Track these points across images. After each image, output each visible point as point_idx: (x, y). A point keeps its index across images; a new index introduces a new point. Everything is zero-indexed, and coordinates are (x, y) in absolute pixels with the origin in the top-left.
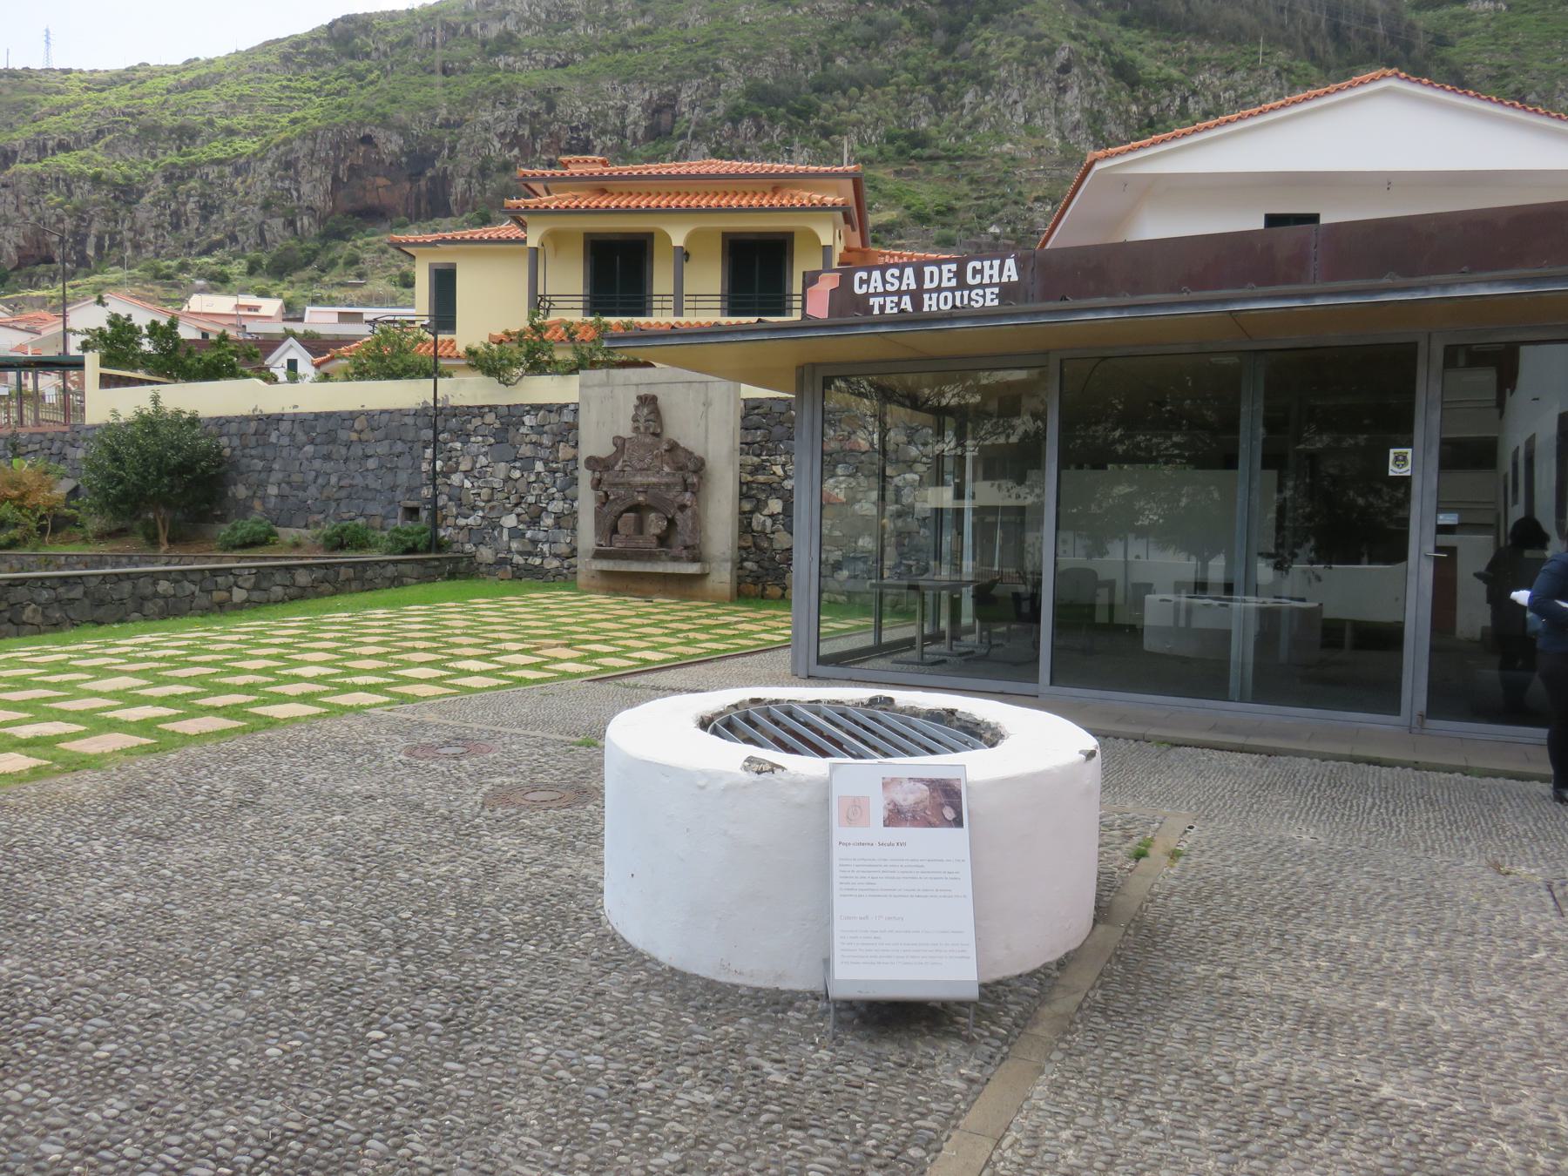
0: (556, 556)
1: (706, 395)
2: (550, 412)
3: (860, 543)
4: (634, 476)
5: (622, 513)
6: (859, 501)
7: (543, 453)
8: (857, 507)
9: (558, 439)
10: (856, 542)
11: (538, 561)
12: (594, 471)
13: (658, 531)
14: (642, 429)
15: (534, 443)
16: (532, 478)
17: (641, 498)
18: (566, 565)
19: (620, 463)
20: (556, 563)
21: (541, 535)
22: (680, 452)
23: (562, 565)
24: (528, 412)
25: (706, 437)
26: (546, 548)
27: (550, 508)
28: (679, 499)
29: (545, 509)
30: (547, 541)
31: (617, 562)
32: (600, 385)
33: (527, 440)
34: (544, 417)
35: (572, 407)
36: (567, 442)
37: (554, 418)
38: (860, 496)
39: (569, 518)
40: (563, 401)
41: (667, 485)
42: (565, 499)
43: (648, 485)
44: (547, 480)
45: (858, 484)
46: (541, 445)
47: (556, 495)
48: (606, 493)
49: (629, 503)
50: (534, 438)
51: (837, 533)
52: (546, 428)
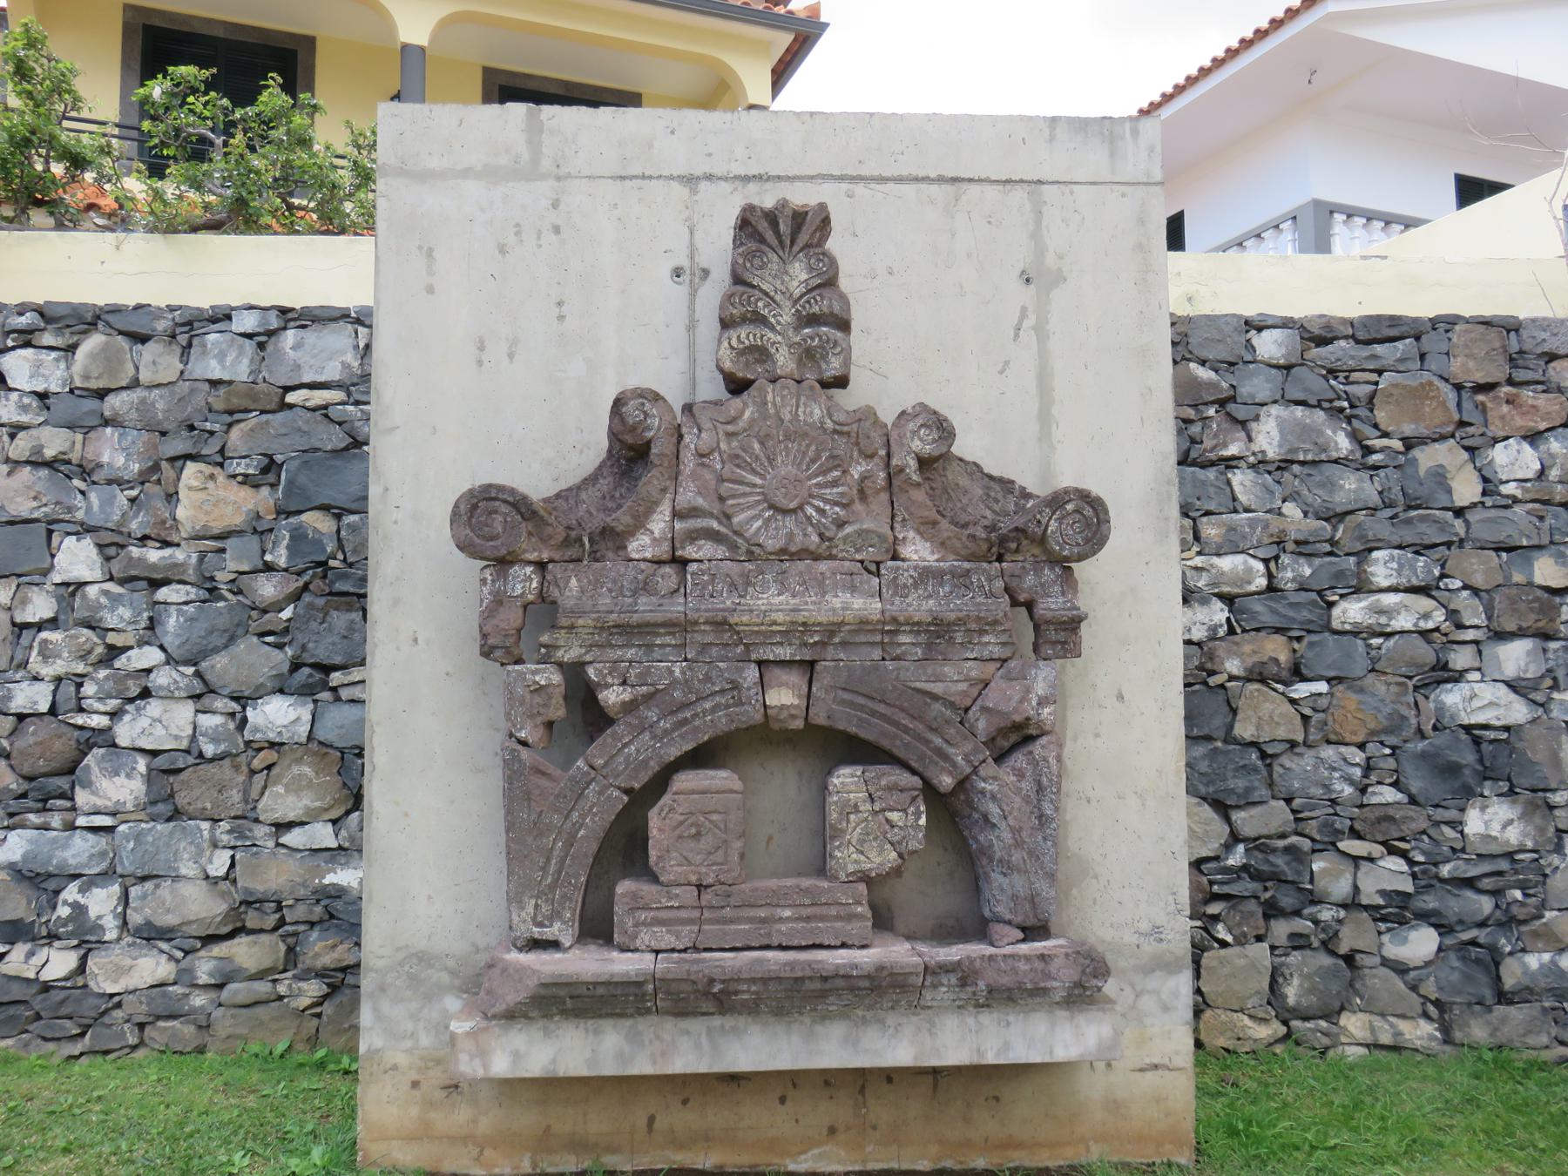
0: (151, 935)
1: (1036, 236)
2: (143, 339)
3: (1475, 822)
4: (742, 585)
5: (660, 783)
6: (1458, 677)
7: (93, 504)
8: (1452, 697)
9: (177, 446)
10: (1456, 825)
11: (58, 963)
12: (503, 563)
13: (881, 858)
14: (784, 360)
15: (49, 464)
16: (40, 606)
17: (784, 696)
18: (204, 967)
19: (659, 523)
20: (152, 967)
21: (79, 850)
22: (954, 474)
23: (185, 977)
24: (26, 339)
25: (1045, 417)
26: (101, 903)
27: (125, 733)
28: (1004, 698)
29: (103, 739)
30: (108, 875)
31: (646, 1025)
32: (490, 174)
33: (21, 447)
34: (108, 358)
35: (247, 322)
36: (221, 459)
37: (157, 362)
38: (1461, 658)
39: (225, 770)
40: (203, 299)
41: (938, 633)
42: (202, 694)
43: (831, 629)
44: (121, 616)
45: (1452, 614)
46: (86, 471)
47: (162, 678)
48: (574, 672)
49: (712, 721)
50: (54, 442)
51: (1388, 795)
52: (114, 403)
